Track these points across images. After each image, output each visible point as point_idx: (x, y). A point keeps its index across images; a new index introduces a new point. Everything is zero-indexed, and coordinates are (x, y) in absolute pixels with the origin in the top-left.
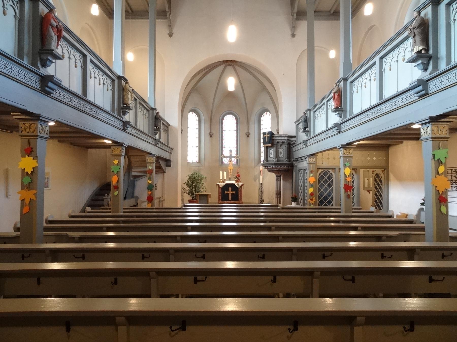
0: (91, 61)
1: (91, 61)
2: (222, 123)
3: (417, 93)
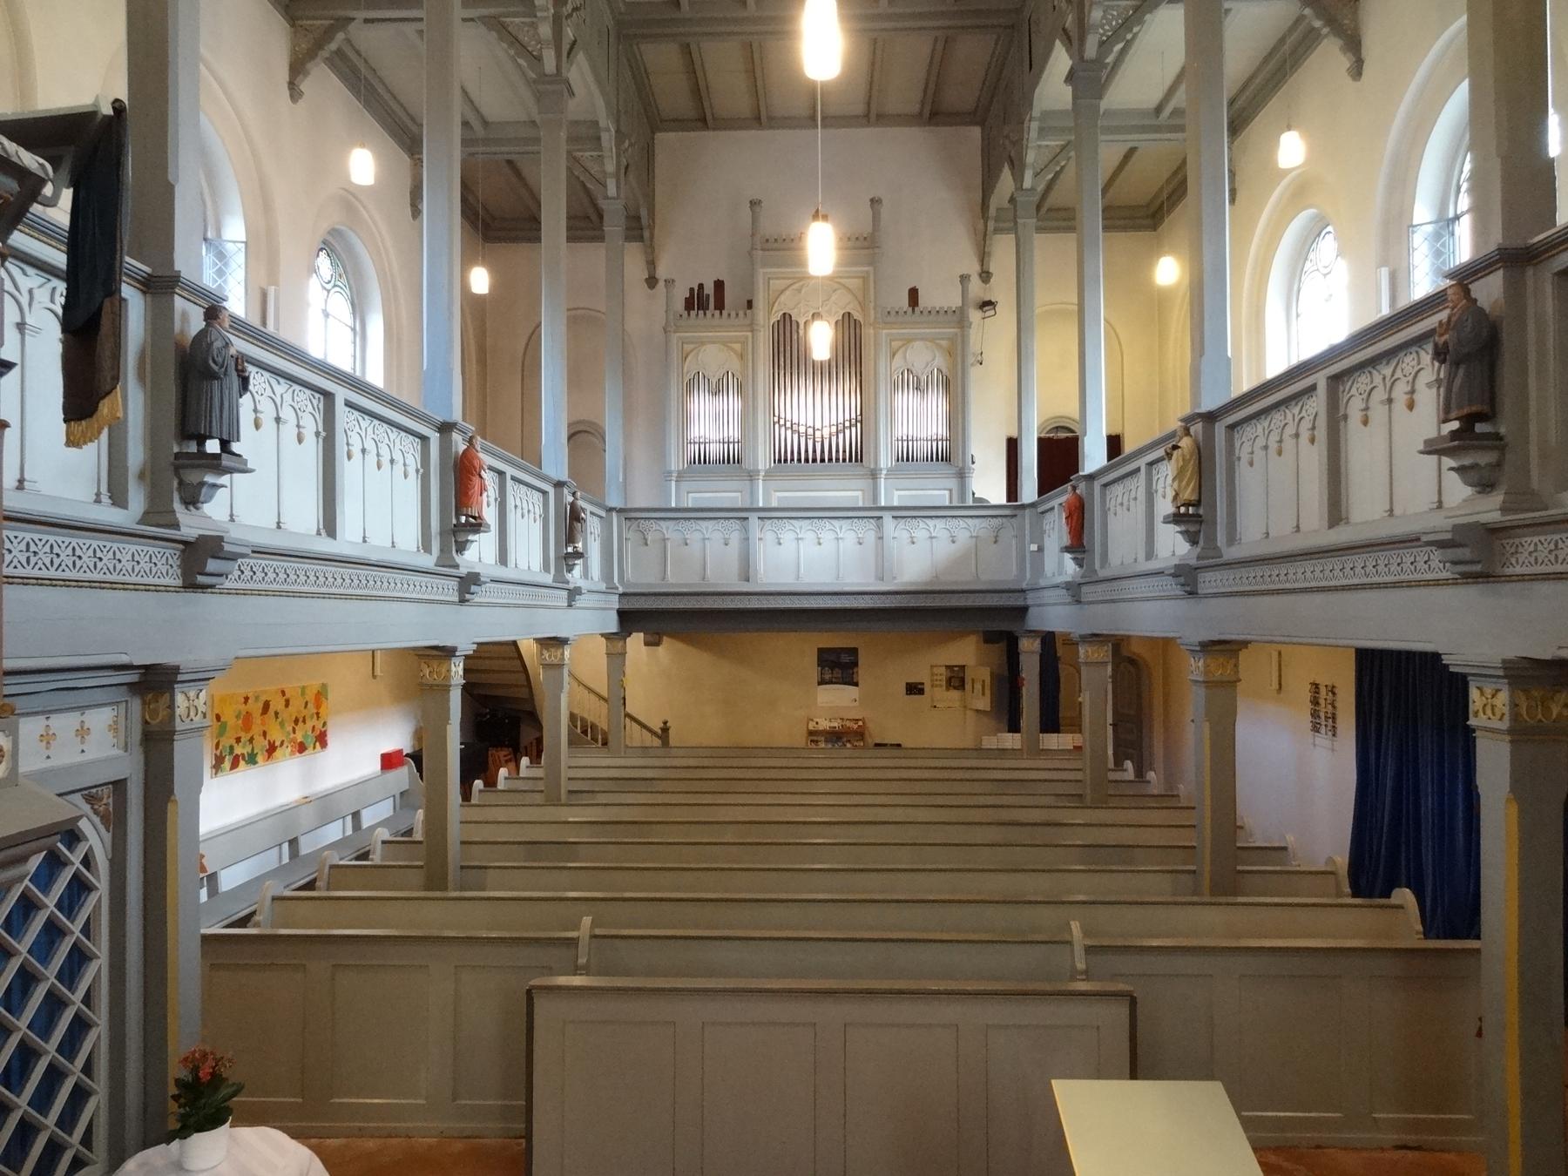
0: (348, 404)
1: (348, 404)
3: (1454, 563)
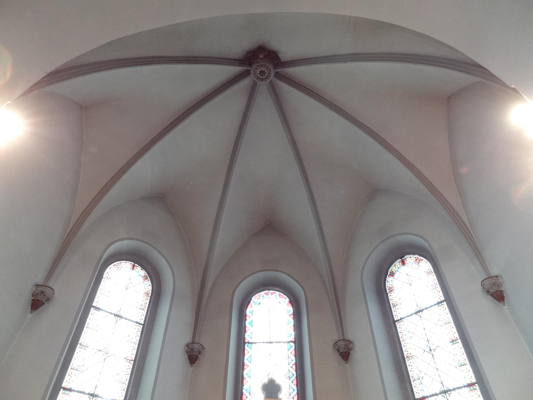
2: (242, 317)
